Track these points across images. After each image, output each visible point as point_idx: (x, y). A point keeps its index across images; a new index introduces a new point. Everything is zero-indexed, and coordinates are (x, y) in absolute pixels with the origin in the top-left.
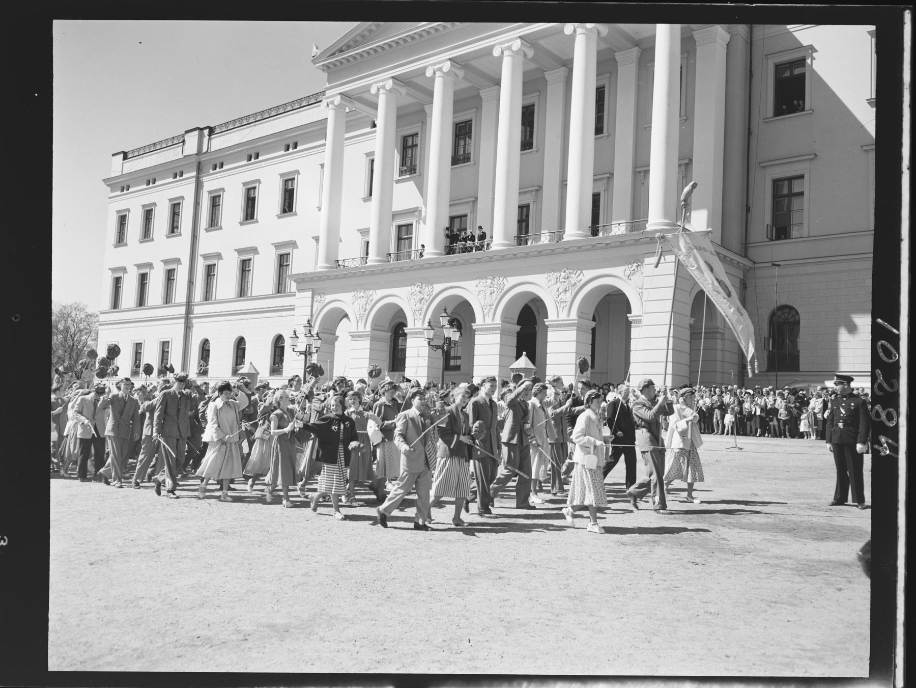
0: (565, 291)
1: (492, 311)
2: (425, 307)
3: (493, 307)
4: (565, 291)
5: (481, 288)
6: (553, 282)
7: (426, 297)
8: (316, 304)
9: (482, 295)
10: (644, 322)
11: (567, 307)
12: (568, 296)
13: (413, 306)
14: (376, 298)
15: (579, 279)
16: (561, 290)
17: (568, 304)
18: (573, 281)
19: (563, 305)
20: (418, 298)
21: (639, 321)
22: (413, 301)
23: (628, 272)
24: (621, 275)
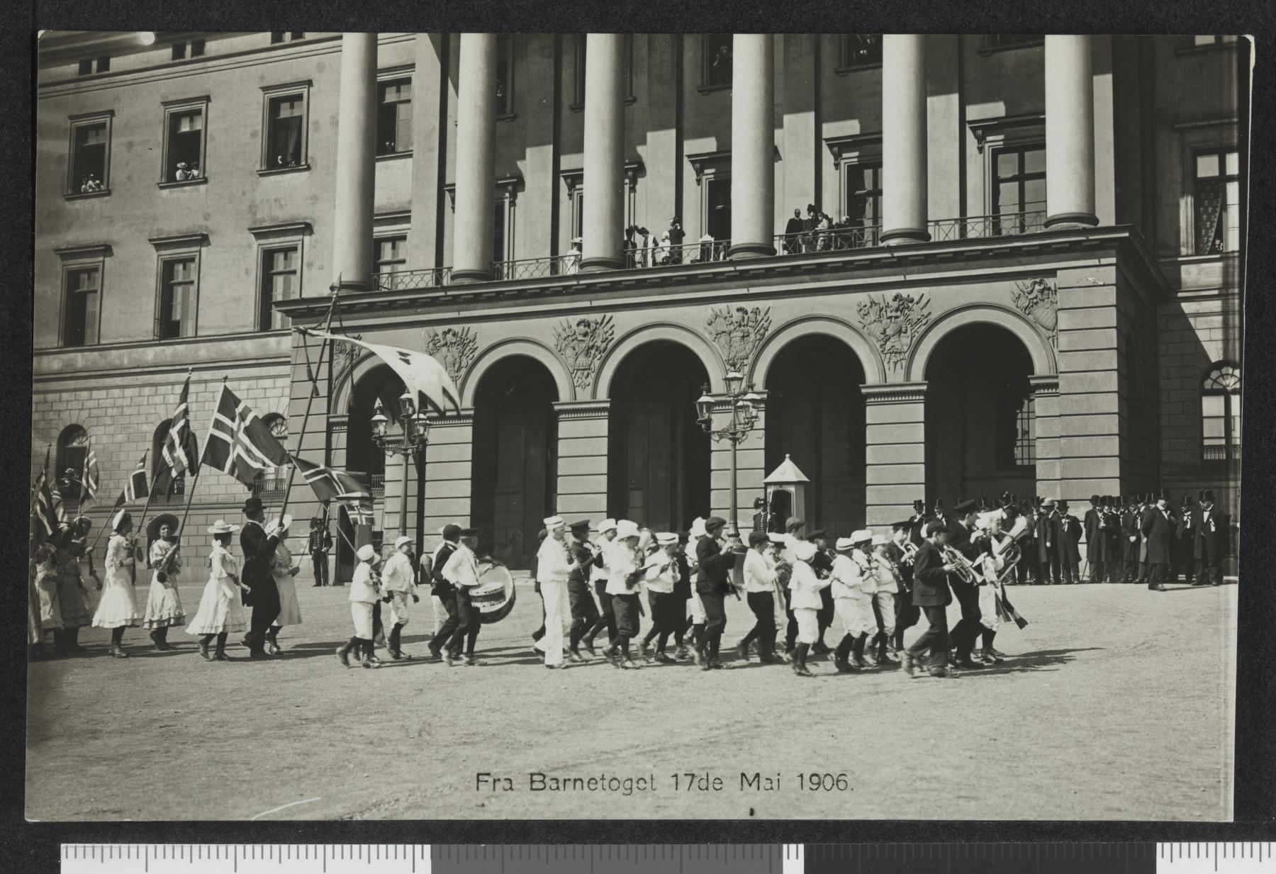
0: (900, 332)
2: (597, 363)
4: (900, 332)
5: (721, 325)
6: (872, 317)
7: (599, 343)
8: (341, 362)
9: (723, 339)
10: (1061, 390)
13: (571, 361)
14: (482, 345)
15: (925, 312)
16: (889, 332)
18: (914, 316)
20: (583, 345)
21: (1056, 386)
22: (569, 352)
23: (1024, 302)
24: (1012, 305)
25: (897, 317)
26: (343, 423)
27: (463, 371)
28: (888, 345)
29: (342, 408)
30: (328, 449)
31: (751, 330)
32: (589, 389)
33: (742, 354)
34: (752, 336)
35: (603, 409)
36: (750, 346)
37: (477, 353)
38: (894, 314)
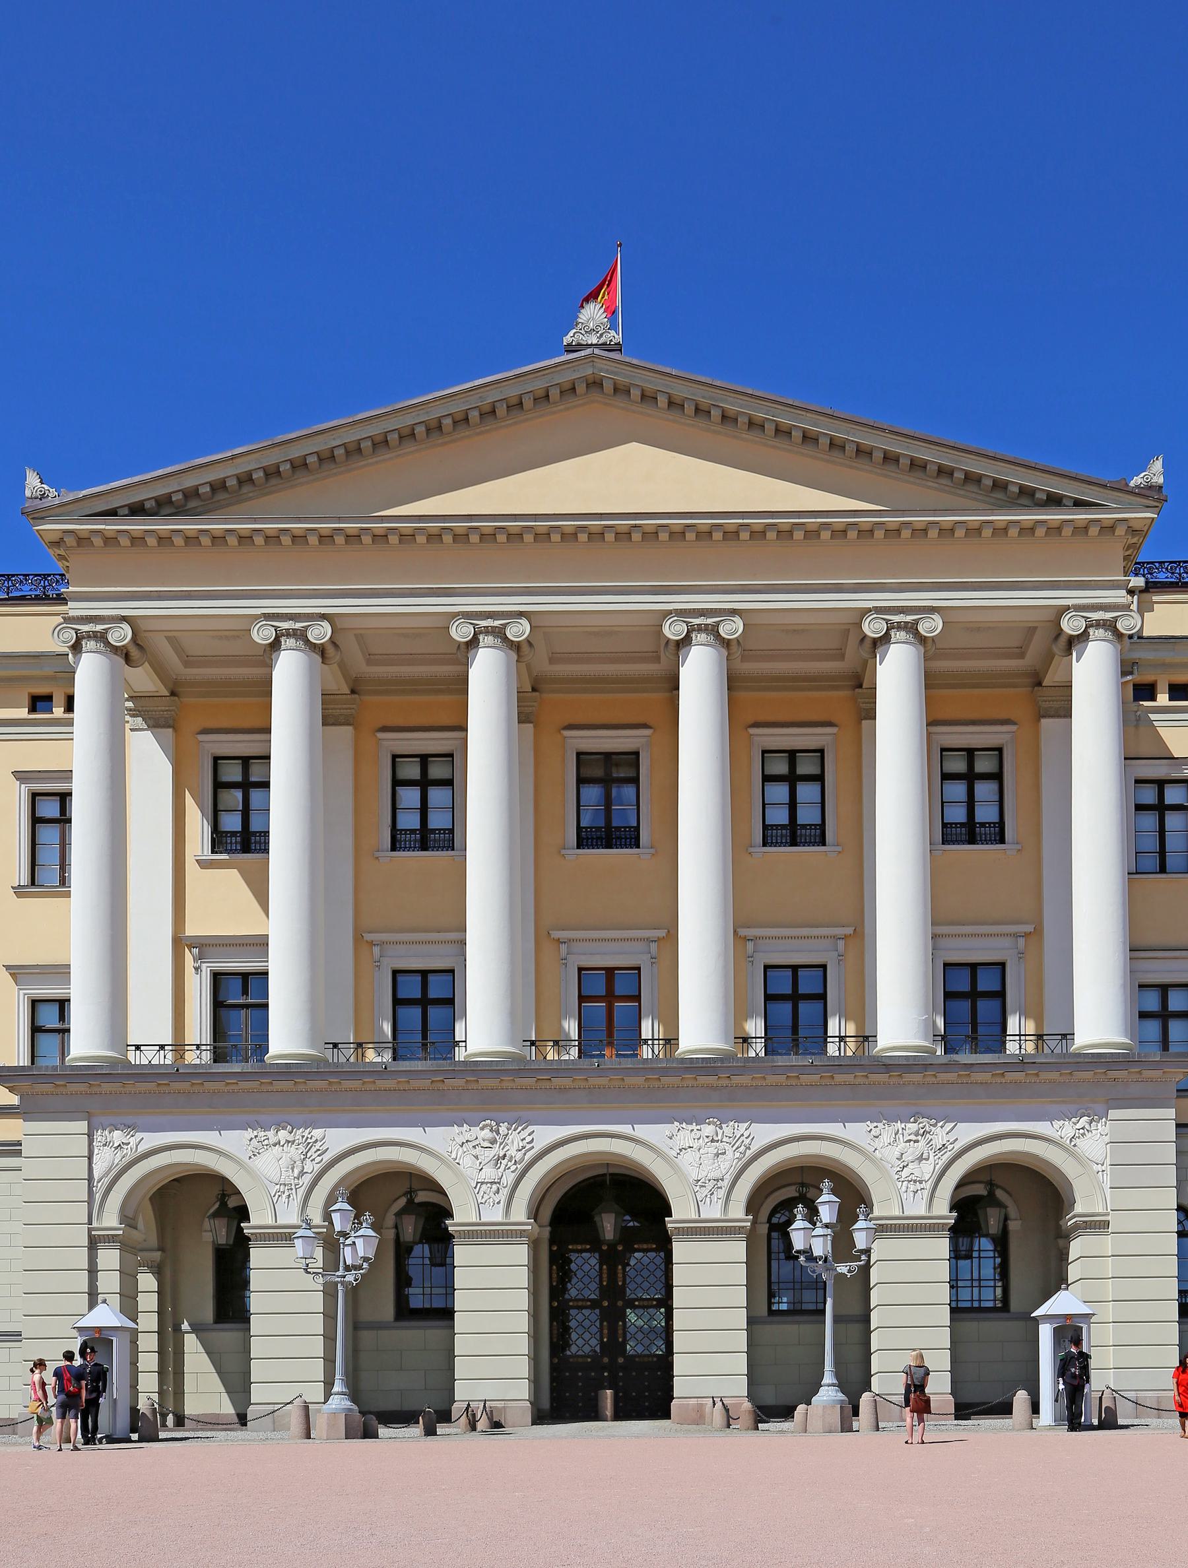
0: (921, 1159)
1: (722, 1193)
3: (726, 1184)
4: (921, 1159)
7: (512, 1152)
11: (926, 1194)
12: (927, 1170)
17: (928, 1186)
18: (938, 1141)
19: (912, 1187)
22: (467, 1161)
25: (915, 1141)
26: (112, 1239)
27: (307, 1180)
28: (905, 1173)
29: (110, 1220)
30: (93, 1271)
31: (727, 1147)
32: (501, 1208)
33: (718, 1175)
34: (730, 1153)
35: (522, 1233)
36: (727, 1165)
37: (327, 1157)
38: (913, 1137)
